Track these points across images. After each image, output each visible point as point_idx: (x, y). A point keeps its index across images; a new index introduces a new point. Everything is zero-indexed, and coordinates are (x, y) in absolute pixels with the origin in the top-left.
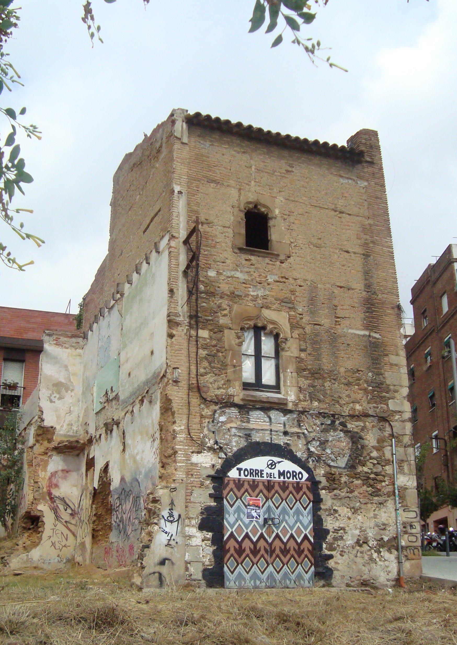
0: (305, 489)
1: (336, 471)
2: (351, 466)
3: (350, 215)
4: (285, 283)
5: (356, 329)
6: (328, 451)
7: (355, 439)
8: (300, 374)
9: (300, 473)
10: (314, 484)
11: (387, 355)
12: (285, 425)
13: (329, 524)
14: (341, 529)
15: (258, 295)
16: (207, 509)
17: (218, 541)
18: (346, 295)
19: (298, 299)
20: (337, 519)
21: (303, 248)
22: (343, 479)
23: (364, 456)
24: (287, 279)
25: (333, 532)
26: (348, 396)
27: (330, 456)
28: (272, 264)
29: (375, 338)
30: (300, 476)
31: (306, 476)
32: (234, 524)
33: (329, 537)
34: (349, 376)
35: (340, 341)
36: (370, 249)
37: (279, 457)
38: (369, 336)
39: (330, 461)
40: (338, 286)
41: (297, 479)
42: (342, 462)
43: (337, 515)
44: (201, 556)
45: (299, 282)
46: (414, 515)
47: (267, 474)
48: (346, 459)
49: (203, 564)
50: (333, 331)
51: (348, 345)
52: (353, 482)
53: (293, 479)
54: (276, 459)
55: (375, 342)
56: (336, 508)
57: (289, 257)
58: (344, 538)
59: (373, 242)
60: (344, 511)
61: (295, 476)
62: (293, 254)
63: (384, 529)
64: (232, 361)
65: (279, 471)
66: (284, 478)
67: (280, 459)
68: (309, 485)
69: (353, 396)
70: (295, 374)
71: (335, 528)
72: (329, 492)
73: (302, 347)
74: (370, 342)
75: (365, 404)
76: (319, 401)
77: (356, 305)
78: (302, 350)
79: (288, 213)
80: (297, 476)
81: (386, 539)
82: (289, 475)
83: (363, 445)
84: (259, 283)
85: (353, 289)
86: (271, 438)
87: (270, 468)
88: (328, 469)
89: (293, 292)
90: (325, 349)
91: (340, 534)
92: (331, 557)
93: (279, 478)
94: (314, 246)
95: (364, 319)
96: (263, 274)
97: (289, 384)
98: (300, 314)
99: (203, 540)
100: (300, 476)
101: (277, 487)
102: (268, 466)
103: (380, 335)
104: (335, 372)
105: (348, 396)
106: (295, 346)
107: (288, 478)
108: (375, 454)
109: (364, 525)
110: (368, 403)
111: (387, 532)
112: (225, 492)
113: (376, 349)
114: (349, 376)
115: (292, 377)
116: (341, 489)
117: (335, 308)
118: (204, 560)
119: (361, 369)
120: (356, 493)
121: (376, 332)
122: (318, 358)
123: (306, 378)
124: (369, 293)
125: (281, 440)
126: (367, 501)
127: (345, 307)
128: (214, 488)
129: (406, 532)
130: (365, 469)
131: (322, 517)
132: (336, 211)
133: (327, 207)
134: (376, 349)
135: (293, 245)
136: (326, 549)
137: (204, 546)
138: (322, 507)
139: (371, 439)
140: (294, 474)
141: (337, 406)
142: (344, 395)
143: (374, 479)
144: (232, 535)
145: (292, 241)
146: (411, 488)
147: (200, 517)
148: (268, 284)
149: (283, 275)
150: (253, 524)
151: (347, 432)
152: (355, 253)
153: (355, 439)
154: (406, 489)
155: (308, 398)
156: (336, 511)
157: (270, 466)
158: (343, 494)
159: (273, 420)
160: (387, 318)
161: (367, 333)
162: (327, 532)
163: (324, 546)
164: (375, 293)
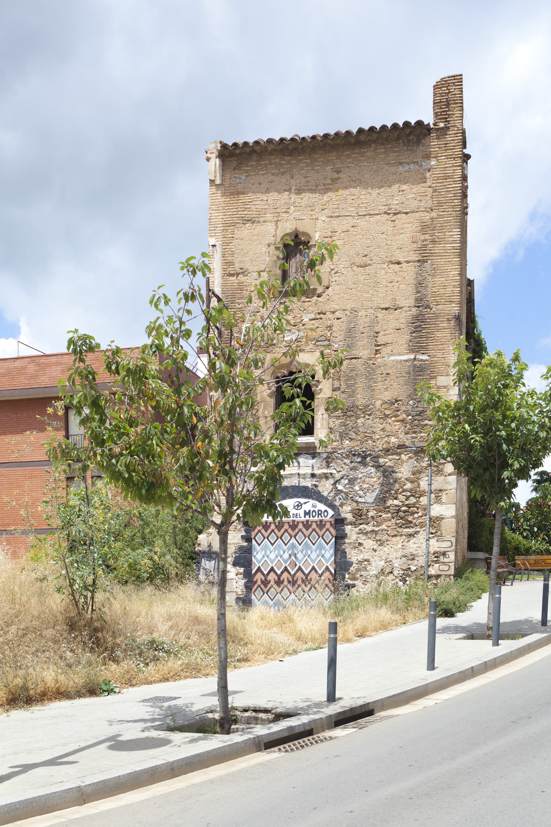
0: (328, 526)
1: (364, 507)
2: (381, 500)
3: (407, 213)
4: (321, 319)
5: (399, 354)
6: (357, 488)
7: (387, 473)
8: (331, 415)
9: (326, 511)
10: (339, 522)
11: (435, 377)
12: (313, 468)
13: (353, 556)
14: (365, 561)
15: (292, 339)
16: (241, 548)
17: (248, 575)
18: (392, 317)
19: (334, 334)
20: (361, 552)
21: (344, 273)
22: (371, 514)
23: (395, 489)
24: (324, 314)
25: (357, 564)
26: (383, 430)
27: (358, 492)
28: (308, 301)
29: (422, 360)
30: (326, 514)
31: (331, 513)
32: (261, 560)
33: (352, 569)
34: (385, 409)
35: (379, 372)
36: (428, 251)
37: (306, 498)
38: (415, 359)
39: (357, 498)
40: (383, 309)
41: (322, 517)
42: (370, 498)
43: (361, 548)
44: (235, 587)
45: (337, 314)
46: (449, 544)
47: (293, 514)
48: (375, 494)
49: (237, 594)
50: (371, 362)
51: (387, 374)
52: (381, 516)
53: (318, 517)
54: (302, 500)
55: (420, 365)
56: (361, 541)
57: (327, 288)
58: (368, 568)
59: (433, 242)
60: (369, 543)
61: (321, 514)
62: (332, 284)
63: (413, 559)
64: (263, 412)
65: (305, 511)
66: (310, 517)
67: (306, 500)
68: (333, 522)
69: (388, 428)
70: (326, 416)
71: (359, 560)
72: (356, 527)
73: (335, 386)
74: (415, 366)
75: (402, 436)
76: (351, 439)
77: (402, 326)
78: (334, 390)
79: (330, 234)
80: (322, 514)
81: (413, 568)
82: (314, 514)
83: (396, 479)
84: (293, 326)
85: (400, 308)
86: (299, 481)
87: (297, 509)
88: (355, 504)
89: (330, 328)
90: (361, 384)
91: (363, 566)
92: (354, 586)
93: (305, 517)
94: (358, 266)
95: (410, 341)
96: (298, 315)
97: (319, 427)
98: (335, 351)
99: (237, 575)
100: (326, 514)
101: (300, 526)
102: (294, 507)
103: (429, 356)
104: (371, 406)
105: (383, 430)
106: (327, 386)
107: (313, 517)
108: (408, 486)
109: (390, 556)
110: (406, 433)
111: (415, 562)
112: (253, 534)
113: (421, 373)
114: (385, 409)
115: (323, 419)
116: (368, 524)
117: (376, 335)
118: (237, 590)
119: (401, 398)
120: (384, 527)
121: (423, 354)
122: (352, 394)
123: (338, 417)
124: (421, 308)
125: (308, 483)
126: (396, 533)
127: (387, 332)
128: (245, 531)
129: (437, 562)
130: (396, 502)
131: (346, 550)
132: (389, 214)
133: (378, 212)
134: (421, 373)
135: (333, 272)
136: (349, 578)
137: (237, 579)
138: (347, 541)
139: (404, 471)
140: (320, 513)
141: (370, 442)
142: (378, 429)
143: (405, 512)
144: (259, 570)
145: (332, 268)
146: (447, 518)
147: (234, 556)
148: (304, 325)
149: (319, 311)
150: (277, 560)
151: (378, 467)
152: (408, 262)
153: (387, 473)
154: (443, 518)
155: (338, 438)
156: (360, 544)
157: (296, 508)
158: (369, 528)
159: (301, 464)
160: (439, 334)
161: (412, 356)
162: (351, 564)
163: (347, 576)
164: (428, 307)
